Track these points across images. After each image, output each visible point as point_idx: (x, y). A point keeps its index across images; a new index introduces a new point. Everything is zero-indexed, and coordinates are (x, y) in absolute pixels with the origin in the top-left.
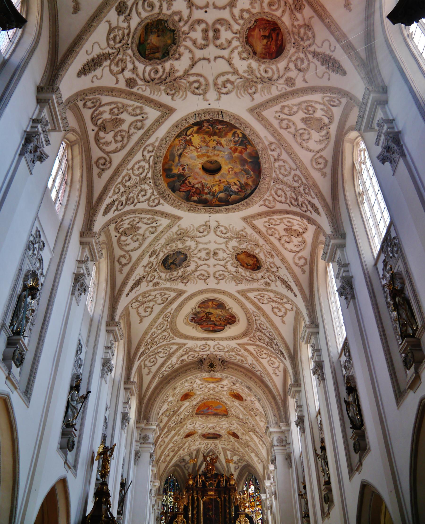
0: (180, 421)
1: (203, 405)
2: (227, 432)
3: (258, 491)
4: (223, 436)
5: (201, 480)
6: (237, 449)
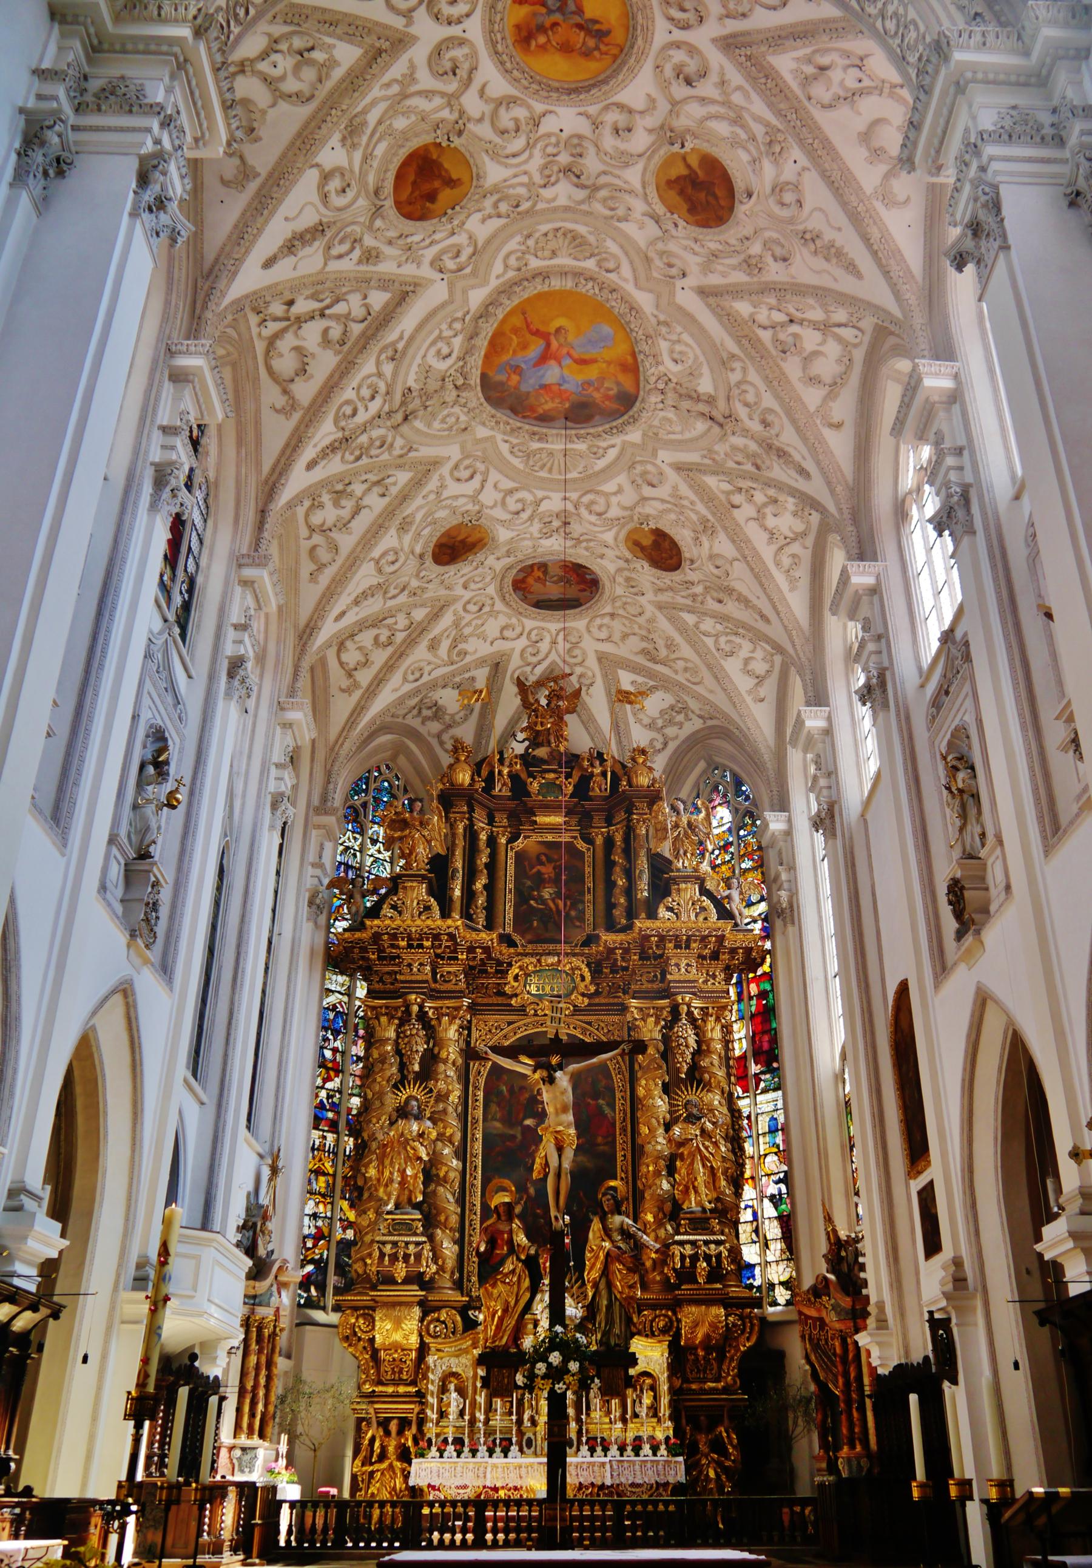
0: (403, 403)
1: (517, 321)
2: (628, 538)
3: (747, 820)
4: (607, 584)
5: (506, 771)
6: (663, 652)
